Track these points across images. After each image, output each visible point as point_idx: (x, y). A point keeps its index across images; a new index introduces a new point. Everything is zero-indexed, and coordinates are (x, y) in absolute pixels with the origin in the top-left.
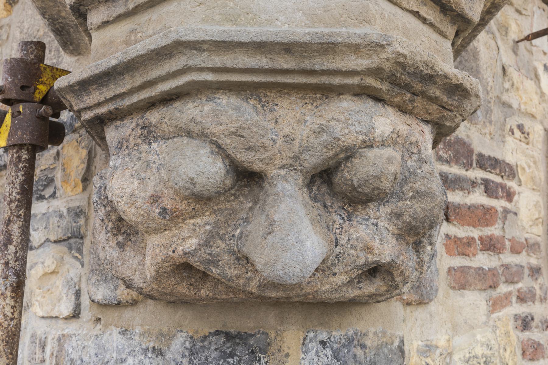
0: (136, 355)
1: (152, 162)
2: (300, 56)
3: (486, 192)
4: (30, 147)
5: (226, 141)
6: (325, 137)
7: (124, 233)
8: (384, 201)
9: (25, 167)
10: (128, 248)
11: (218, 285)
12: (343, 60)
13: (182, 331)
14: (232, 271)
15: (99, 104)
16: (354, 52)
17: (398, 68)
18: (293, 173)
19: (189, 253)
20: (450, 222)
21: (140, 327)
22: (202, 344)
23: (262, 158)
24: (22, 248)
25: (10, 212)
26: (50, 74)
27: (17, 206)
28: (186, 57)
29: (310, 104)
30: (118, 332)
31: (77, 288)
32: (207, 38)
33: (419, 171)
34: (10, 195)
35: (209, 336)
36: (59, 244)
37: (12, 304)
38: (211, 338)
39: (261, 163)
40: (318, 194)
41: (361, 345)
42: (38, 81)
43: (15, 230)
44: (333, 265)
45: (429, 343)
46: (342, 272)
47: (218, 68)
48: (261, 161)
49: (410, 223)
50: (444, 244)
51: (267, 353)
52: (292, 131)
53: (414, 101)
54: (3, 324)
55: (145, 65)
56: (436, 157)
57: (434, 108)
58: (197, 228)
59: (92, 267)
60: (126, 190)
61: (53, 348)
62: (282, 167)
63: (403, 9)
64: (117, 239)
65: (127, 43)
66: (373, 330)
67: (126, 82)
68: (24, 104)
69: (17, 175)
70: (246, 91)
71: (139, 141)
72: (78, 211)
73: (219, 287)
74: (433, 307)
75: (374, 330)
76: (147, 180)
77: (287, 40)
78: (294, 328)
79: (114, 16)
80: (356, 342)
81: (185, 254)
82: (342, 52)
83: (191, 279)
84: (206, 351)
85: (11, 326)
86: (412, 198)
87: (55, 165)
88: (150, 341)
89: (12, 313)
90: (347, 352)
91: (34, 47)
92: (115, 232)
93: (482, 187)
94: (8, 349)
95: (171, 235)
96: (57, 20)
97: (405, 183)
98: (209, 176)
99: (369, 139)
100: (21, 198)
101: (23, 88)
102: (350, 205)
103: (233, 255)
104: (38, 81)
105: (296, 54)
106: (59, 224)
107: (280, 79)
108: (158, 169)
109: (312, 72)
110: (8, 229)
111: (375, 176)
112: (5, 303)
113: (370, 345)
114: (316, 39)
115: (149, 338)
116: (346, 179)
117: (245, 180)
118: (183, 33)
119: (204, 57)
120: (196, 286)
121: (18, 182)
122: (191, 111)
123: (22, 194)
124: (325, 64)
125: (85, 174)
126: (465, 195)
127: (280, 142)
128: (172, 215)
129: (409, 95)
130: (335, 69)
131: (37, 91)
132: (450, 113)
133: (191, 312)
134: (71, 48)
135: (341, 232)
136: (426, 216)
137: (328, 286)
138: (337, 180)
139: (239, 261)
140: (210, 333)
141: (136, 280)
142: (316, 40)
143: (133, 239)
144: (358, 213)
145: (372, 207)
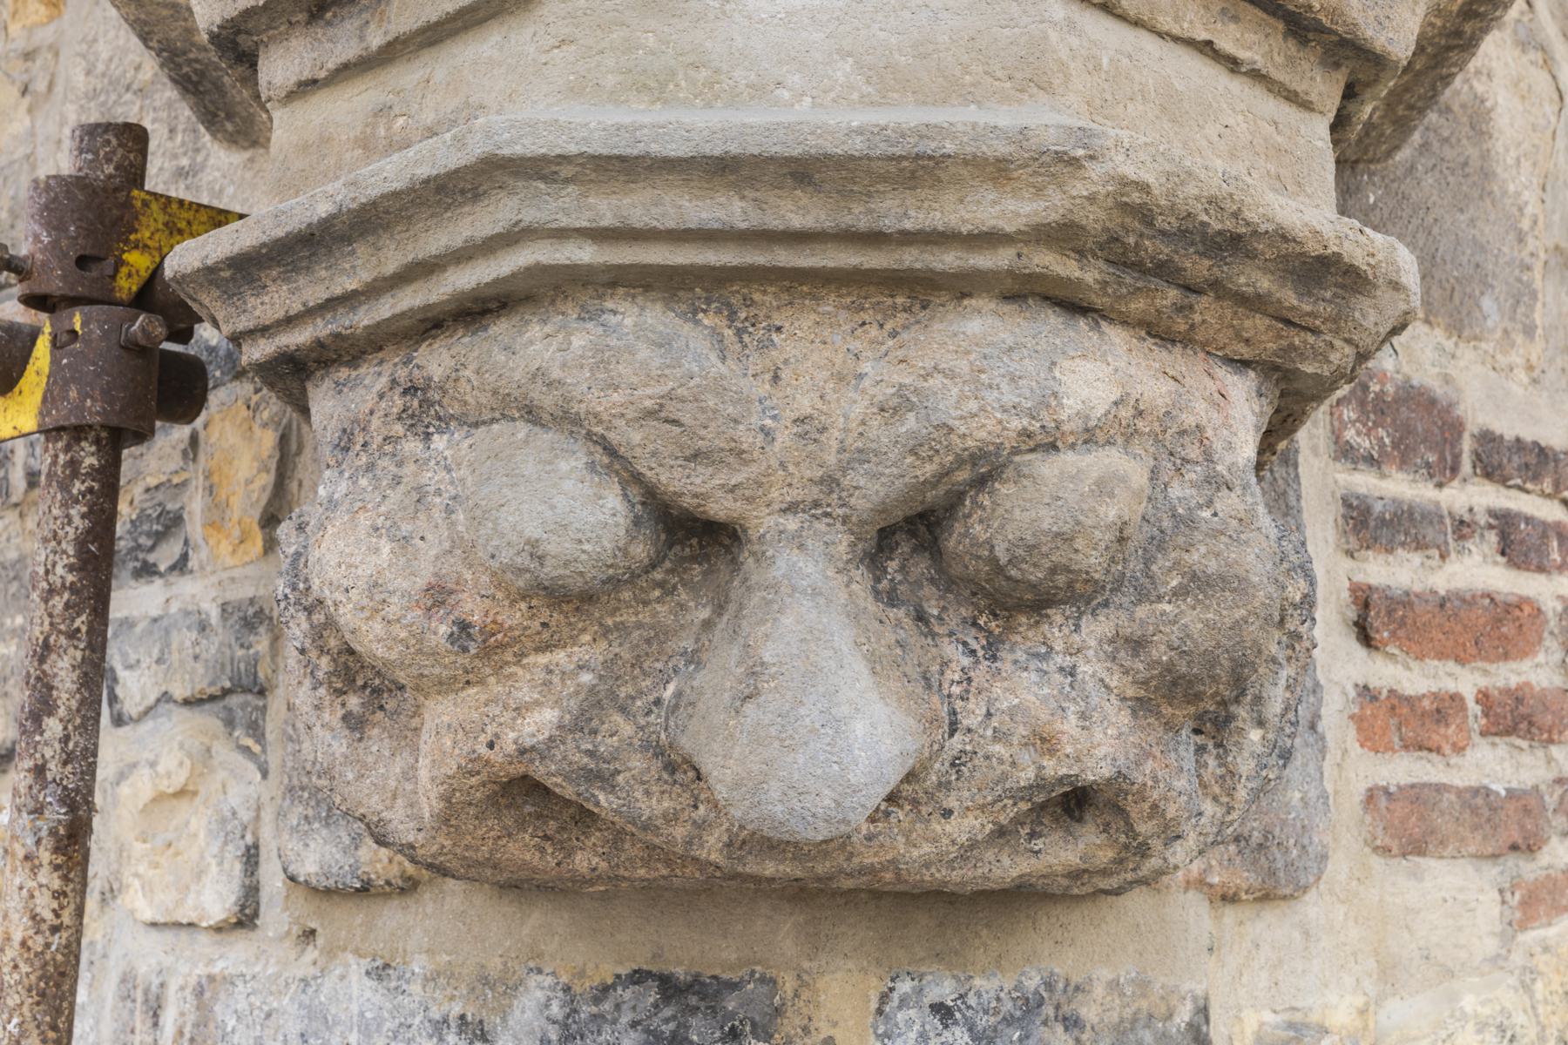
0: (413, 1039)
1: (431, 489)
2: (838, 192)
3: (1503, 553)
4: (104, 434)
5: (630, 437)
6: (911, 421)
7: (364, 687)
8: (1095, 602)
9: (90, 490)
10: (376, 731)
11: (623, 841)
12: (962, 202)
13: (540, 971)
14: (654, 801)
15: (289, 321)
16: (994, 180)
17: (1128, 220)
18: (821, 526)
19: (533, 748)
20: (1377, 649)
21: (424, 956)
22: (594, 1010)
23: (733, 482)
24: (83, 725)
25: (47, 623)
26: (162, 218)
27: (67, 606)
28: (516, 198)
29: (875, 325)
30: (363, 971)
31: (249, 839)
32: (572, 149)
33: (1206, 514)
34: (47, 572)
35: (613, 986)
36: (197, 710)
37: (56, 887)
38: (619, 991)
39: (730, 496)
40: (900, 582)
41: (1065, 1019)
42: (126, 242)
43: (63, 673)
44: (944, 786)
45: (1298, 1017)
46: (968, 808)
47: (606, 229)
48: (732, 491)
49: (1169, 668)
50: (1352, 717)
51: (771, 1036)
52: (819, 405)
53: (1191, 307)
54: (30, 943)
55: (409, 218)
56: (1333, 447)
57: (1257, 325)
58: (556, 679)
59: (290, 778)
60: (360, 572)
61: (182, 1014)
62: (791, 508)
63: (1161, 35)
64: (343, 705)
65: (366, 145)
66: (1106, 974)
67: (360, 262)
68: (87, 309)
69: (68, 516)
70: (692, 289)
71: (399, 429)
72: (251, 611)
73: (627, 846)
74: (1312, 907)
75: (1111, 977)
76: (417, 541)
77: (796, 152)
78: (850, 965)
79: (331, 65)
80: (1048, 1010)
81: (522, 751)
82: (958, 181)
83: (545, 823)
84: (607, 1028)
85: (53, 948)
86: (1180, 593)
87: (184, 476)
88: (452, 998)
89: (54, 911)
90: (1020, 1040)
91: (114, 142)
92: (339, 685)
93: (1493, 537)
94: (45, 1013)
95: (483, 697)
96: (185, 53)
97: (1160, 548)
98: (580, 535)
99: (1043, 427)
100: (80, 580)
101: (82, 262)
102: (995, 616)
103: (656, 755)
104: (126, 242)
105: (827, 187)
106: (197, 650)
107: (784, 257)
108: (449, 511)
109: (875, 238)
110: (44, 672)
111: (1057, 535)
112: (34, 884)
113: (1096, 1020)
114: (882, 145)
115: (449, 991)
116: (975, 543)
117: (694, 541)
118: (506, 136)
119: (567, 199)
120: (561, 842)
121: (71, 536)
122: (536, 348)
123: (80, 569)
124: (912, 213)
125: (269, 503)
126: (1429, 562)
127: (784, 438)
128: (484, 641)
129: (1173, 294)
130: (941, 228)
131: (124, 270)
132: (1311, 339)
133: (566, 916)
134: (229, 127)
135: (967, 691)
136: (1218, 645)
137: (927, 848)
138: (952, 543)
139: (673, 773)
140: (618, 976)
141: (395, 822)
142: (882, 148)
143: (391, 705)
144: (1018, 638)
145: (1059, 619)
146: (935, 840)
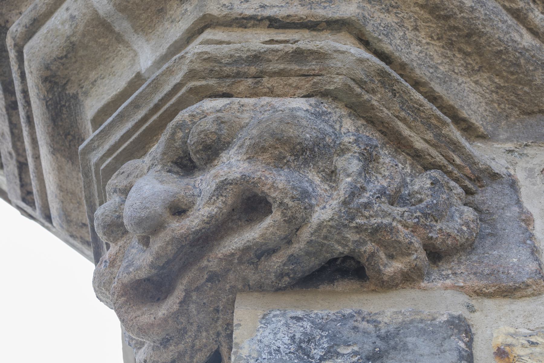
47: (109, 150)
109: (157, 107)
129: (250, 81)
132: (320, 78)
137: (197, 221)
146: (198, 217)
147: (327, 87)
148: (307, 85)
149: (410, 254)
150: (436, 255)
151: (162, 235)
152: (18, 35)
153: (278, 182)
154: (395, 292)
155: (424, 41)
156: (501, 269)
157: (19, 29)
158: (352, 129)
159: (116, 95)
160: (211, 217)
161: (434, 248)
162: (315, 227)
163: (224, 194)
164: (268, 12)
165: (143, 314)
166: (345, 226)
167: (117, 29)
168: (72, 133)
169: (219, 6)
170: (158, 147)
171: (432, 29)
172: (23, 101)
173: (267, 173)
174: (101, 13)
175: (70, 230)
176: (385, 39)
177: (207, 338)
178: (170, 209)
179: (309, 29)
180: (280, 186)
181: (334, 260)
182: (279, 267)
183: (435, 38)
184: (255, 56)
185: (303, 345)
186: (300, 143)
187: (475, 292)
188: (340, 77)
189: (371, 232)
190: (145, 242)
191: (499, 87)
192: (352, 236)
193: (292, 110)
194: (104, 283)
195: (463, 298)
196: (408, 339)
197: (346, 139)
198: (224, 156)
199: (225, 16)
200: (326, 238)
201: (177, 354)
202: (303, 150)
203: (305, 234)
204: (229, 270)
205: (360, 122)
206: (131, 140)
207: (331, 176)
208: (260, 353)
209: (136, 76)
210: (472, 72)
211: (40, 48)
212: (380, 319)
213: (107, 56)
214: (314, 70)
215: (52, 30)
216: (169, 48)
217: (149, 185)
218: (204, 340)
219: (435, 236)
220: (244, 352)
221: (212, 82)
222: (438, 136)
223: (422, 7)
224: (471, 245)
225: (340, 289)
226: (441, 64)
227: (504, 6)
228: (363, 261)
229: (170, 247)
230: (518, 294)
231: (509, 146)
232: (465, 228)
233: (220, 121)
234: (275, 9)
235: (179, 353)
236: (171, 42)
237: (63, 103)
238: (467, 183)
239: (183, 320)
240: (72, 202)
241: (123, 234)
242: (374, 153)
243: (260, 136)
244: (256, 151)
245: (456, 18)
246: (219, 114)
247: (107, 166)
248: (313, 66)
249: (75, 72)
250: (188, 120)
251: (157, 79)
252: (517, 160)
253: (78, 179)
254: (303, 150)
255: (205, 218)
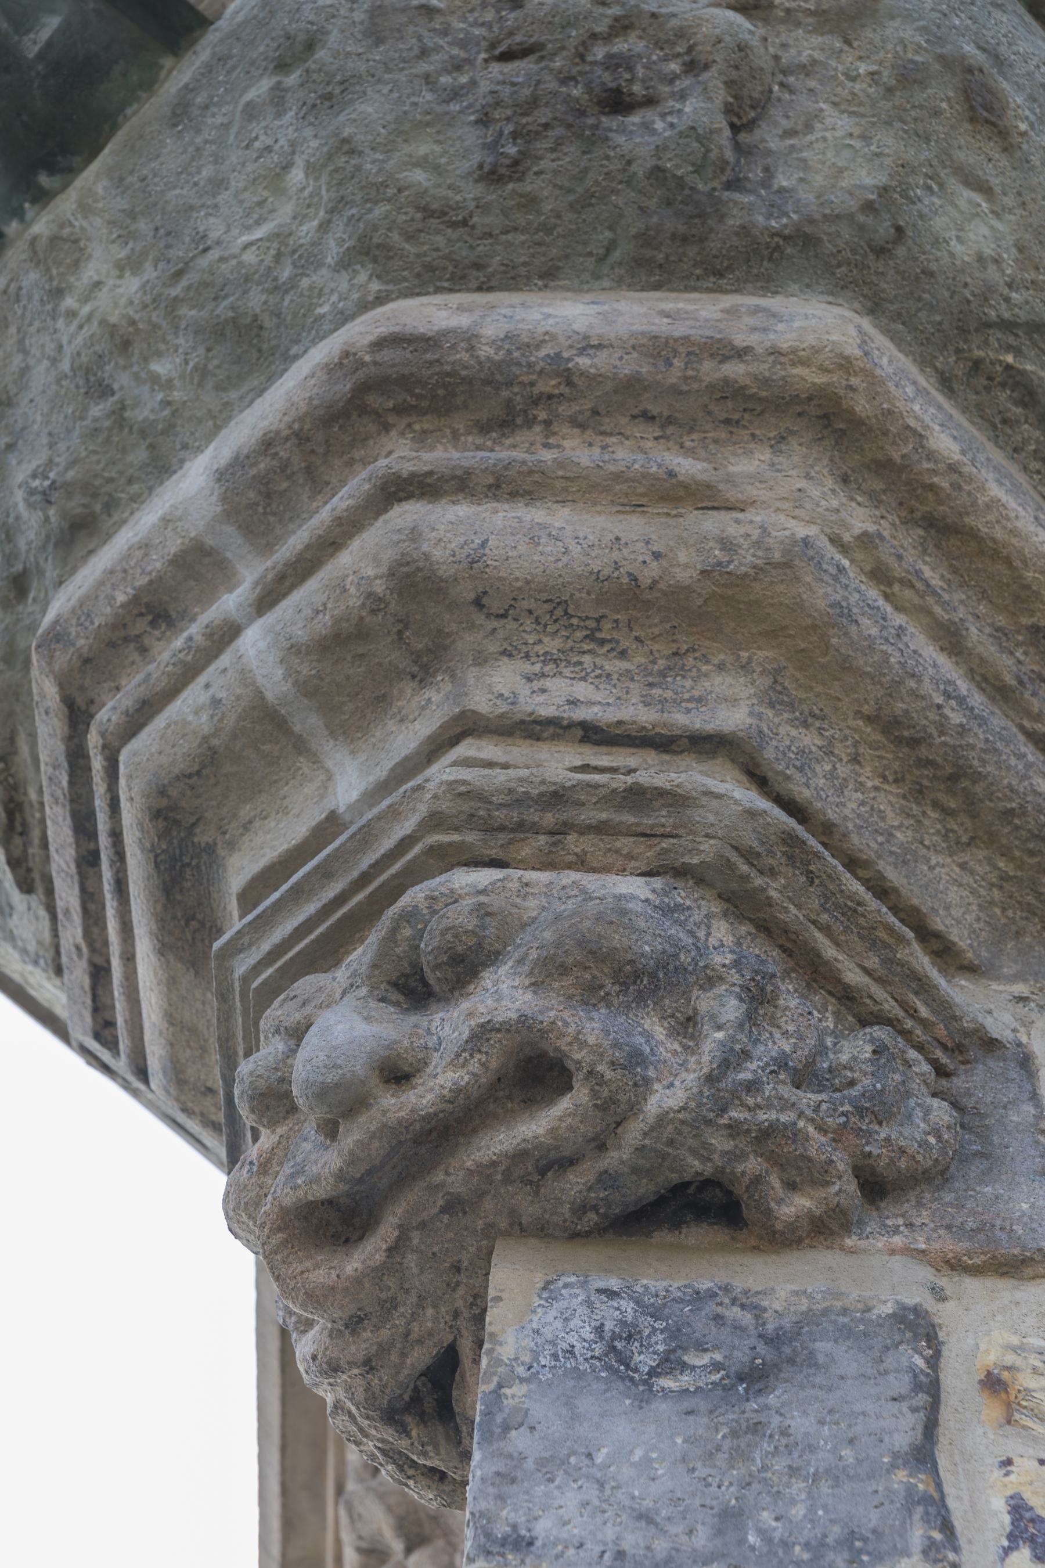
47: (269, 953)
109: (365, 878)
129: (542, 839)
132: (675, 841)
137: (430, 1097)
146: (432, 1090)
147: (686, 859)
148: (648, 853)
149: (827, 1184)
150: (875, 1187)
151: (362, 1119)
152: (111, 728)
153: (587, 1031)
154: (796, 1254)
155: (869, 784)
156: (998, 1222)
157: (114, 718)
158: (729, 940)
159: (288, 850)
160: (457, 1091)
161: (873, 1172)
162: (651, 1120)
163: (484, 1050)
164: (581, 714)
165: (317, 1267)
166: (709, 1122)
167: (297, 728)
168: (199, 917)
169: (490, 696)
170: (364, 953)
171: (885, 762)
172: (111, 852)
173: (566, 1015)
174: (270, 696)
175: (183, 1098)
176: (797, 776)
177: (435, 1320)
178: (381, 1070)
179: (656, 749)
180: (591, 1040)
181: (681, 1187)
182: (580, 1192)
183: (891, 778)
184: (555, 794)
185: (619, 1345)
186: (631, 962)
187: (947, 1262)
188: (712, 842)
189: (756, 1137)
190: (330, 1130)
191: (1005, 878)
192: (720, 1143)
193: (619, 898)
194: (246, 1204)
195: (924, 1273)
196: (819, 1345)
197: (718, 959)
198: (487, 978)
199: (502, 716)
200: (671, 1142)
201: (375, 1348)
202: (637, 975)
203: (633, 1133)
204: (484, 1193)
205: (744, 929)
206: (313, 936)
207: (687, 1027)
208: (535, 1355)
209: (327, 818)
210: (955, 845)
211: (152, 755)
212: (765, 1303)
213: (275, 778)
214: (663, 826)
215: (176, 723)
216: (392, 770)
217: (343, 1025)
218: (429, 1324)
219: (876, 1152)
220: (506, 1352)
221: (471, 837)
222: (889, 962)
223: (869, 719)
224: (942, 1173)
225: (691, 1241)
226: (899, 827)
227: (1021, 728)
228: (739, 1190)
229: (376, 1144)
230: (1029, 1271)
231: (1020, 989)
232: (932, 1140)
233: (483, 912)
234: (596, 709)
235: (380, 1345)
236: (398, 759)
237: (186, 860)
238: (939, 1054)
239: (391, 1282)
240: (189, 1046)
241: (288, 1112)
242: (769, 988)
243: (558, 944)
244: (547, 972)
245: (930, 745)
246: (482, 899)
247: (264, 983)
248: (662, 818)
249: (214, 803)
250: (423, 906)
251: (368, 824)
252: (1034, 1016)
253: (203, 1003)
254: (637, 975)
255: (446, 1092)
